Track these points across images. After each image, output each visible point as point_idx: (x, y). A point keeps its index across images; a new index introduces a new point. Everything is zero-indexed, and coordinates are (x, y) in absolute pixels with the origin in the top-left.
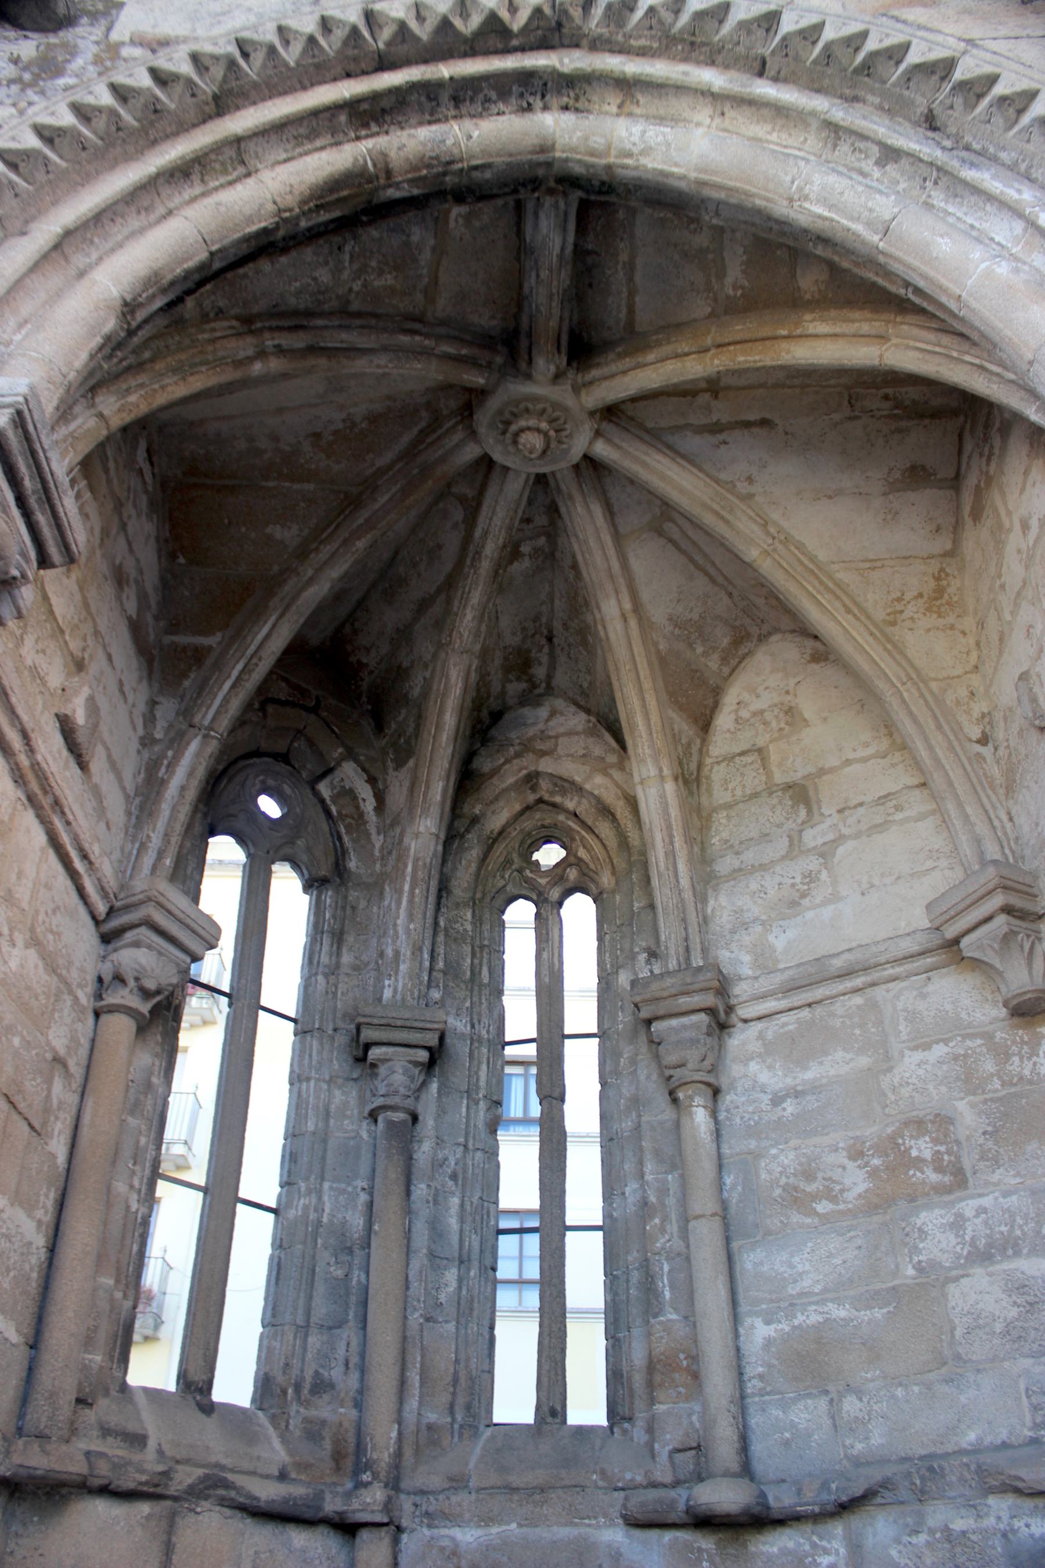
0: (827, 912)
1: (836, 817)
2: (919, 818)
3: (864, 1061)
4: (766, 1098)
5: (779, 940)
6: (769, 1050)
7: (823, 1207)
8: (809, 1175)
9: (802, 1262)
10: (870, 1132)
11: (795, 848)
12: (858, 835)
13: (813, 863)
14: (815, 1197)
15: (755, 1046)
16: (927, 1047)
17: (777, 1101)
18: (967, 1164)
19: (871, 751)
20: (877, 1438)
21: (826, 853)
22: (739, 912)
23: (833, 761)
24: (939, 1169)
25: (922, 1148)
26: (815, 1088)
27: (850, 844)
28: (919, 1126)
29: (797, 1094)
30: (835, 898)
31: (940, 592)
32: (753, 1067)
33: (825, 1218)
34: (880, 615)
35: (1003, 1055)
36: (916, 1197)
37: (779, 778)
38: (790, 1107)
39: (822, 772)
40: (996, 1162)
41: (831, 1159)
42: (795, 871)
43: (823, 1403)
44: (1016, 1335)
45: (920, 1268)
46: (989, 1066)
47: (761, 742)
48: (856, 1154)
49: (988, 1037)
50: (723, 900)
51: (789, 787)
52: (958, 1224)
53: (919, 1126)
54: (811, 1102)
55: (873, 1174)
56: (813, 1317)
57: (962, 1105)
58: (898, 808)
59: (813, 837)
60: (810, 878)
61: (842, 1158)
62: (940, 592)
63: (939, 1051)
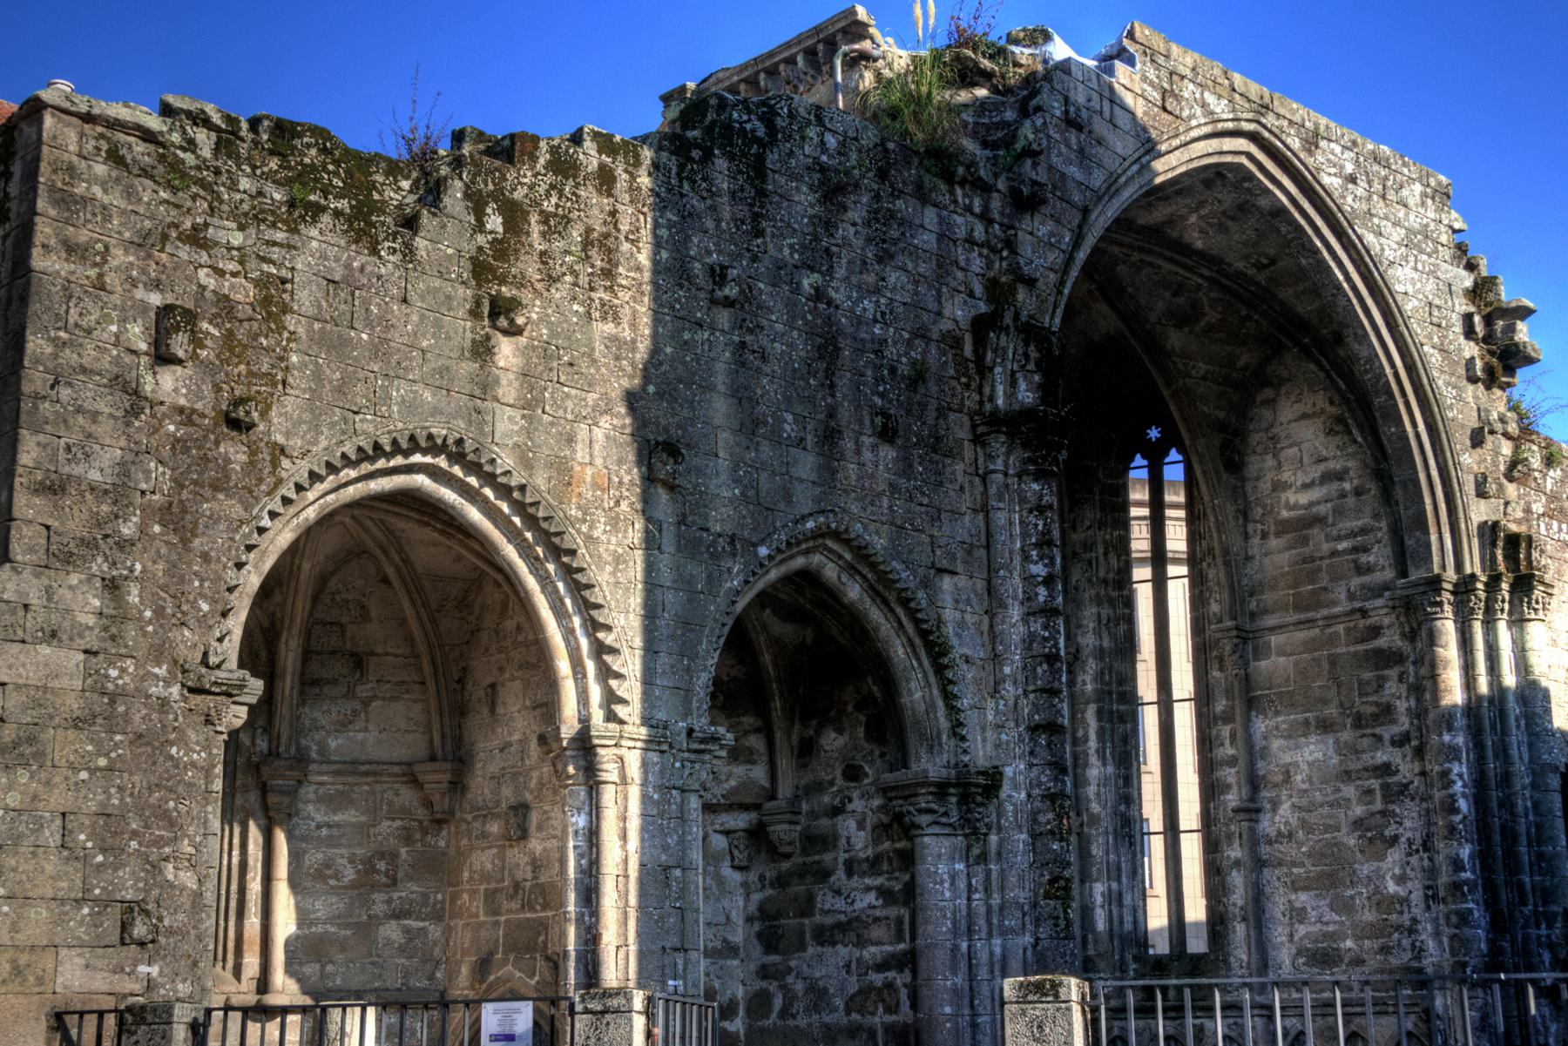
0: (360, 736)
1: (374, 684)
2: (415, 701)
3: (363, 819)
4: (313, 824)
5: (333, 743)
6: (319, 800)
7: (332, 882)
8: (328, 867)
9: (318, 905)
10: (360, 851)
11: (349, 695)
12: (384, 699)
13: (358, 706)
14: (330, 877)
15: (312, 796)
16: (393, 819)
17: (319, 827)
18: (400, 875)
19: (400, 652)
20: (338, 982)
21: (366, 703)
22: (315, 720)
23: (380, 650)
24: (387, 876)
25: (381, 866)
26: (338, 825)
27: (380, 702)
28: (382, 855)
29: (329, 826)
30: (366, 730)
31: (465, 598)
32: (310, 807)
33: (332, 887)
34: (434, 606)
35: (425, 832)
36: (374, 887)
37: (348, 646)
38: (324, 832)
39: (373, 654)
40: (411, 879)
41: (340, 861)
42: (348, 707)
43: (318, 966)
44: (402, 950)
45: (370, 917)
46: (418, 836)
47: (345, 620)
48: (351, 861)
49: (421, 822)
50: (307, 710)
51: (353, 655)
52: (389, 902)
53: (382, 855)
54: (335, 832)
55: (358, 872)
56: (320, 929)
57: (403, 851)
58: (407, 692)
59: (362, 691)
60: (355, 713)
61: (345, 862)
62: (465, 598)
63: (398, 823)
